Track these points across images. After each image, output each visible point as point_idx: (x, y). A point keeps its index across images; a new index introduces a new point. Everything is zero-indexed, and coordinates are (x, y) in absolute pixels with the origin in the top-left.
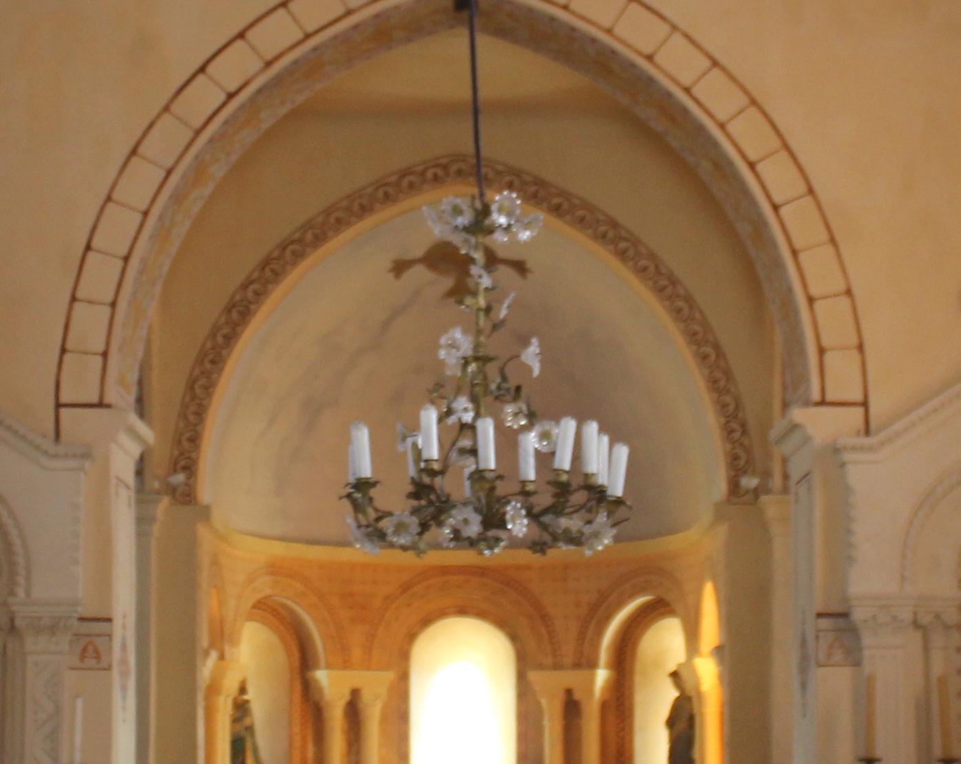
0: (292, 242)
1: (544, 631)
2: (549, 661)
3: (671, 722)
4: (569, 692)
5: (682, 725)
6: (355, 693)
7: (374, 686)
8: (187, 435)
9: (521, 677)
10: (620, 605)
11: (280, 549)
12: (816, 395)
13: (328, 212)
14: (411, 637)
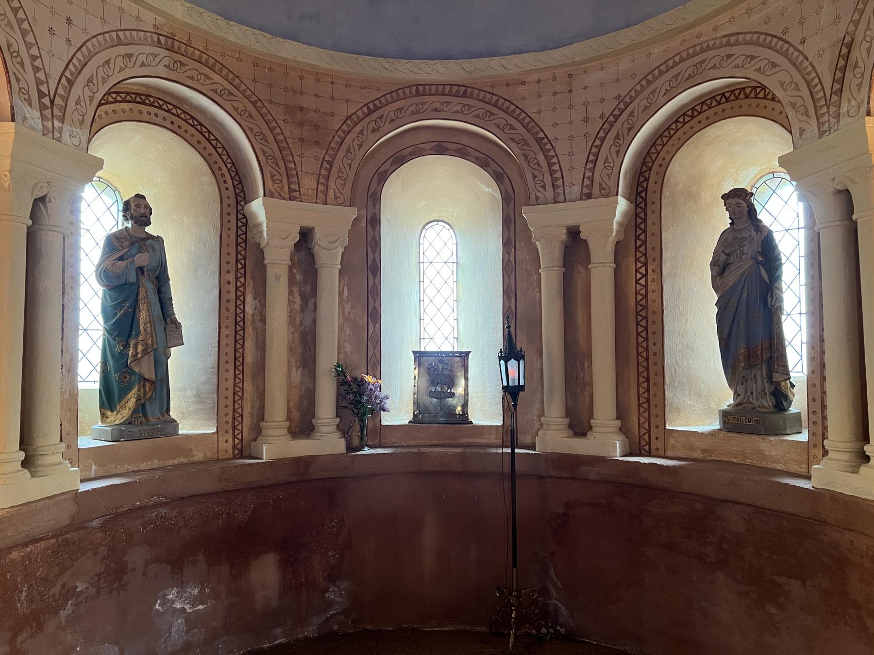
1: (541, 158)
2: (549, 193)
4: (574, 233)
6: (306, 235)
10: (651, 110)
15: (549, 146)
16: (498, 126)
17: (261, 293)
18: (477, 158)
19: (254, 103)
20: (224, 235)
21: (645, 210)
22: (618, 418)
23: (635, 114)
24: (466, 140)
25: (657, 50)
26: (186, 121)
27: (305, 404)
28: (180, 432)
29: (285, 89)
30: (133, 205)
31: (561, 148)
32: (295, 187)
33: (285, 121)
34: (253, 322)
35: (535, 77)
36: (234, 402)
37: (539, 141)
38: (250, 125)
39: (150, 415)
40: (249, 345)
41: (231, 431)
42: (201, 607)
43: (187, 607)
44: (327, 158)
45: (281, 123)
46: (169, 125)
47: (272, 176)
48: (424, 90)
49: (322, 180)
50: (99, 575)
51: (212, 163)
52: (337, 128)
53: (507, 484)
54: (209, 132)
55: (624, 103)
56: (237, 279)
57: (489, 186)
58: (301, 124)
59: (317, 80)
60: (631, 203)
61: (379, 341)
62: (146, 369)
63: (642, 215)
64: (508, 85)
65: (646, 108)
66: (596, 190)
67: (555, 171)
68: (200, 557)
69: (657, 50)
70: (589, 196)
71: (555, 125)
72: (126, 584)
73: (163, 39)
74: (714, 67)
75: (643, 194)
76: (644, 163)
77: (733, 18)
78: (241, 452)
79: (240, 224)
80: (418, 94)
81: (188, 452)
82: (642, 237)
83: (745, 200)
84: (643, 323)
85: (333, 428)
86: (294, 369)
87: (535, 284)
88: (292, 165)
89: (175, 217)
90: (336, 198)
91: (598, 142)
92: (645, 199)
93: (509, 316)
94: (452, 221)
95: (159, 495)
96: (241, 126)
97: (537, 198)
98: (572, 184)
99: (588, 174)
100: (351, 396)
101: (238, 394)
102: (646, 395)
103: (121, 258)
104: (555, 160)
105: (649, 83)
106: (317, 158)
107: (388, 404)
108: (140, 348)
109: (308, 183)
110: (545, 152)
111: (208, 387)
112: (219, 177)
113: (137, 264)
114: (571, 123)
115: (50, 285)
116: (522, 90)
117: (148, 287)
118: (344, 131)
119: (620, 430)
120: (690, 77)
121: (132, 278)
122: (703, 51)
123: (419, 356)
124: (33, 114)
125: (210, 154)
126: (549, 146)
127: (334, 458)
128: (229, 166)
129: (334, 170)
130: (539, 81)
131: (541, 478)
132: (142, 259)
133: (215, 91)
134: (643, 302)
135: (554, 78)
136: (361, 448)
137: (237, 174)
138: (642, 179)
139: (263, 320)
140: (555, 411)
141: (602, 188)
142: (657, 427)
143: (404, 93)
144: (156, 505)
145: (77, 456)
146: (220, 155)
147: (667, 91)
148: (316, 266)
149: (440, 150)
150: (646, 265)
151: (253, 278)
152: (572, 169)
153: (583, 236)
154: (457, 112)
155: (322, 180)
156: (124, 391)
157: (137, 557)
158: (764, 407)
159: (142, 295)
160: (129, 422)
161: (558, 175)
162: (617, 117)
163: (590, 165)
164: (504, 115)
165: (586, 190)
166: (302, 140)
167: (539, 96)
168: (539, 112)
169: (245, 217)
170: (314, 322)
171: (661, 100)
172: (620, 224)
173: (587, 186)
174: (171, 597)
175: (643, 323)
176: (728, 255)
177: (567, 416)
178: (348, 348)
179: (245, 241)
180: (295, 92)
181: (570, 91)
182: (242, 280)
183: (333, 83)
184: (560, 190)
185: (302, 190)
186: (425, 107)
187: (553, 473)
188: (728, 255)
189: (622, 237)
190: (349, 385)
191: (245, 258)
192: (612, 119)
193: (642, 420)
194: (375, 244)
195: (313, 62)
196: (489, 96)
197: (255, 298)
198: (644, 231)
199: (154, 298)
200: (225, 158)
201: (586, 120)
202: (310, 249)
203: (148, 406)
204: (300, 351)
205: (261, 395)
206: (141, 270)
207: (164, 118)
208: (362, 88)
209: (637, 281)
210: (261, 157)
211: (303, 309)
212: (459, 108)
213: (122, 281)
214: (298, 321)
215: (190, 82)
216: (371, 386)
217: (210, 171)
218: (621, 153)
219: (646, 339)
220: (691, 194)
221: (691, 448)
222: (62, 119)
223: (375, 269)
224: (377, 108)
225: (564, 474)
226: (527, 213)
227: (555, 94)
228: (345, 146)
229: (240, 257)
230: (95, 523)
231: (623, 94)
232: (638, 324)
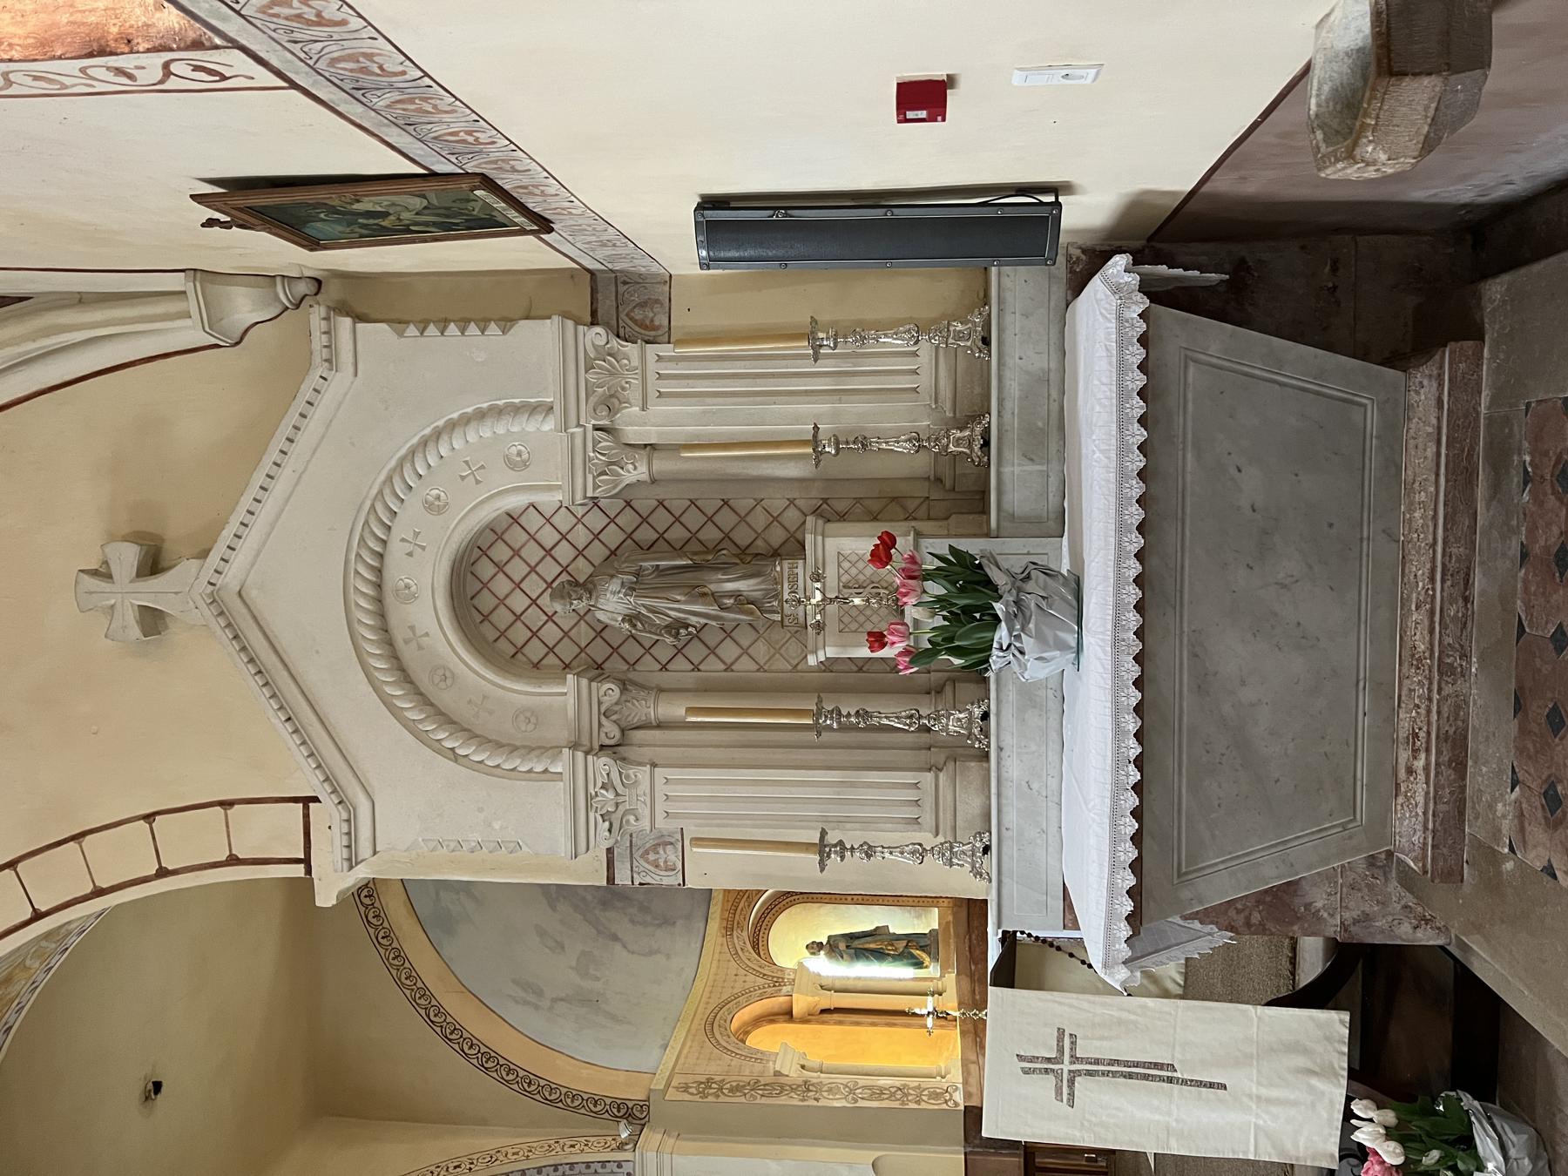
0: (428, 1016)
8: (591, 1106)
11: (714, 925)
12: (298, 869)
13: (401, 985)
62: (901, 945)
113: (844, 948)
115: (860, 985)
117: (857, 943)
124: (785, 989)
132: (842, 946)
144: (970, 939)
145: (942, 976)
156: (913, 956)
160: (929, 954)
199: (863, 940)
206: (847, 947)
230: (973, 967)
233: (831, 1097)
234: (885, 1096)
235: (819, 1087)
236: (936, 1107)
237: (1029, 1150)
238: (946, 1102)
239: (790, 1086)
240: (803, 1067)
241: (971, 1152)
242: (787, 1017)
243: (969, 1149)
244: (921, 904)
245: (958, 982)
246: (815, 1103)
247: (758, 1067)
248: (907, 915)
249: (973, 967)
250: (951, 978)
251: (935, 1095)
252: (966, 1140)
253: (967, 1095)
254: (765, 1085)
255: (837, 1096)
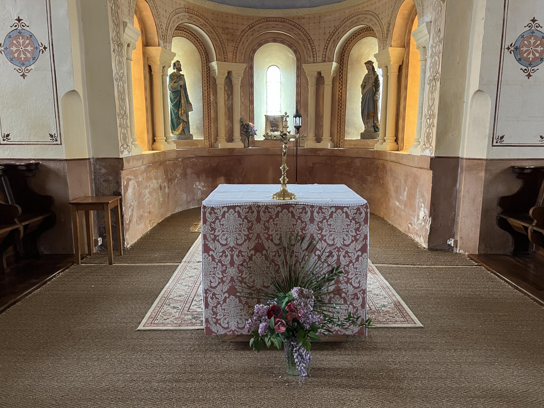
1: (309, 46)
2: (312, 60)
3: (363, 87)
4: (319, 73)
5: (369, 86)
6: (229, 73)
7: (238, 69)
9: (299, 69)
10: (344, 32)
14: (254, 51)
15: (312, 42)
16: (295, 34)
17: (215, 94)
18: (288, 44)
19: (212, 28)
20: (203, 74)
21: (343, 66)
22: (330, 136)
23: (340, 33)
24: (284, 37)
25: (347, 11)
26: (190, 34)
27: (230, 132)
28: (194, 139)
29: (222, 22)
30: (177, 65)
31: (316, 43)
32: (226, 57)
33: (222, 33)
34: (213, 104)
35: (308, 16)
36: (209, 130)
37: (309, 40)
38: (212, 36)
39: (186, 133)
40: (212, 111)
41: (208, 139)
42: (204, 189)
43: (201, 188)
44: (236, 46)
45: (221, 34)
46: (186, 37)
47: (219, 53)
48: (269, 19)
49: (235, 54)
50: (181, 174)
51: (198, 49)
52: (239, 34)
53: (295, 158)
54: (197, 38)
55: (336, 29)
56: (207, 89)
57: (292, 54)
58: (227, 34)
59: (232, 17)
60: (338, 63)
61: (253, 111)
63: (342, 68)
64: (299, 19)
65: (343, 31)
66: (327, 59)
67: (314, 51)
68: (204, 175)
69: (347, 11)
70: (325, 61)
71: (314, 34)
72: (187, 178)
73: (186, 9)
74: (362, 21)
75: (342, 61)
76: (343, 49)
77: (367, 5)
78: (211, 146)
79: (208, 70)
80: (267, 21)
81: (197, 145)
82: (341, 76)
83: (371, 65)
84: (340, 105)
85: (240, 140)
86: (226, 121)
87: (307, 91)
88: (225, 49)
89: (186, 67)
90: (239, 60)
91: (328, 42)
92: (343, 62)
93: (298, 102)
94: (279, 66)
95: (194, 155)
96: (209, 36)
97: (308, 61)
98: (319, 56)
99: (324, 53)
100: (245, 130)
101: (209, 128)
102: (339, 129)
103: (175, 82)
104: (314, 47)
105: (344, 22)
106: (232, 46)
107: (257, 132)
108: (183, 111)
109: (230, 55)
110: (311, 44)
111: (200, 125)
112: (201, 53)
113: (180, 84)
114: (319, 34)
116: (303, 21)
118: (241, 36)
119: (331, 140)
120: (356, 23)
121: (179, 89)
122: (360, 14)
123: (267, 117)
124: (161, 42)
125: (198, 46)
126: (312, 42)
127: (240, 150)
128: (204, 49)
129: (238, 50)
130: (309, 18)
131: (306, 156)
133: (201, 25)
134: (340, 98)
135: (315, 17)
136: (249, 147)
137: (206, 52)
138: (342, 55)
139: (216, 103)
140: (311, 135)
141: (328, 59)
142: (342, 139)
143: (262, 21)
144: (193, 158)
146: (201, 46)
147: (349, 26)
148: (232, 84)
149: (275, 41)
150: (342, 85)
151: (212, 89)
152: (319, 51)
153: (322, 75)
154: (281, 28)
155: (235, 54)
156: (178, 125)
157: (189, 171)
158: (371, 131)
159: (182, 94)
160: (180, 134)
161: (315, 53)
162: (334, 34)
163: (325, 50)
164: (297, 30)
165: (323, 59)
166: (228, 40)
167: (309, 24)
168: (309, 29)
169: (209, 67)
170: (232, 104)
171: (348, 29)
172: (334, 71)
173: (324, 58)
174: (197, 184)
175: (340, 105)
176: (365, 83)
177: (315, 137)
178: (243, 114)
179: (209, 76)
180: (225, 22)
181: (320, 23)
182: (209, 89)
183: (238, 18)
184: (315, 58)
185: (228, 58)
186: (270, 26)
187: (309, 154)
188: (365, 83)
189: (335, 76)
190: (244, 126)
191: (210, 82)
192: (332, 34)
193: (338, 137)
194: (252, 76)
195: (232, 12)
196: (292, 22)
197: (213, 96)
198: (342, 74)
200: (202, 46)
201: (324, 33)
202: (230, 78)
203: (185, 130)
204: (228, 114)
205: (217, 129)
207: (194, 41)
208: (248, 19)
209: (339, 91)
210: (215, 47)
211: (228, 99)
212: (281, 26)
213: (176, 90)
214: (227, 104)
215: (194, 23)
216: (251, 126)
217: (198, 51)
218: (335, 47)
219: (341, 110)
220: (358, 61)
221: (351, 145)
222: (166, 43)
223: (252, 85)
224: (253, 27)
225: (313, 154)
226: (304, 66)
227: (314, 23)
228: (242, 41)
229: (208, 81)
231: (336, 26)
232: (338, 105)
233: (117, 62)
234: (121, 102)
235: (120, 54)
236: (119, 138)
237: (105, 205)
238: (122, 145)
239: (119, 31)
240: (129, 45)
241: (90, 162)
242: (145, 43)
243: (92, 161)
244: (205, 130)
245: (174, 151)
246: (112, 50)
247: (126, 11)
248: (199, 122)
249: (180, 159)
250: (173, 147)
251: (125, 139)
252: (98, 159)
253: (128, 159)
254: (117, 12)
255: (117, 67)
